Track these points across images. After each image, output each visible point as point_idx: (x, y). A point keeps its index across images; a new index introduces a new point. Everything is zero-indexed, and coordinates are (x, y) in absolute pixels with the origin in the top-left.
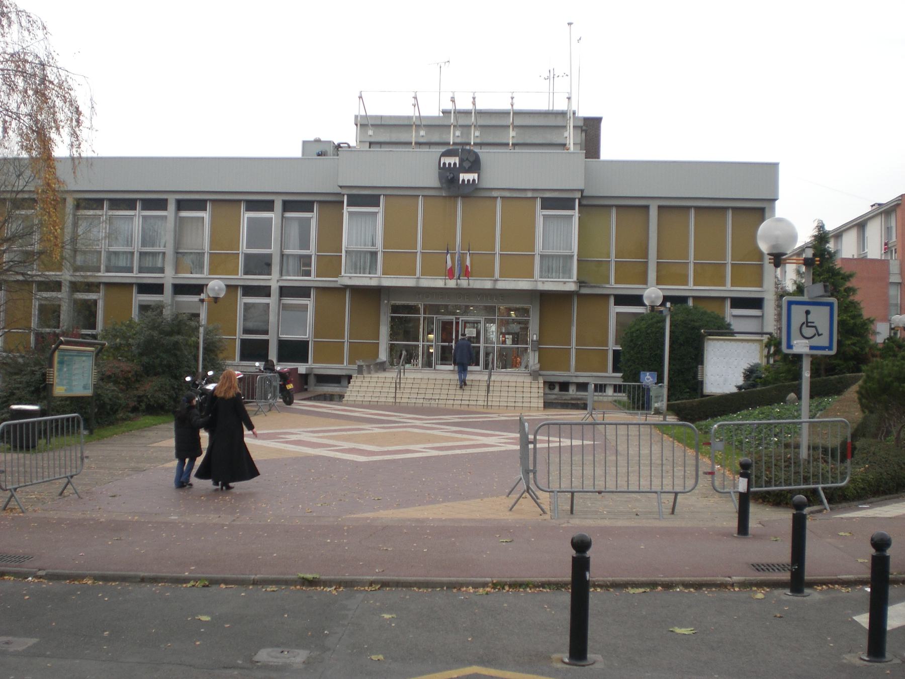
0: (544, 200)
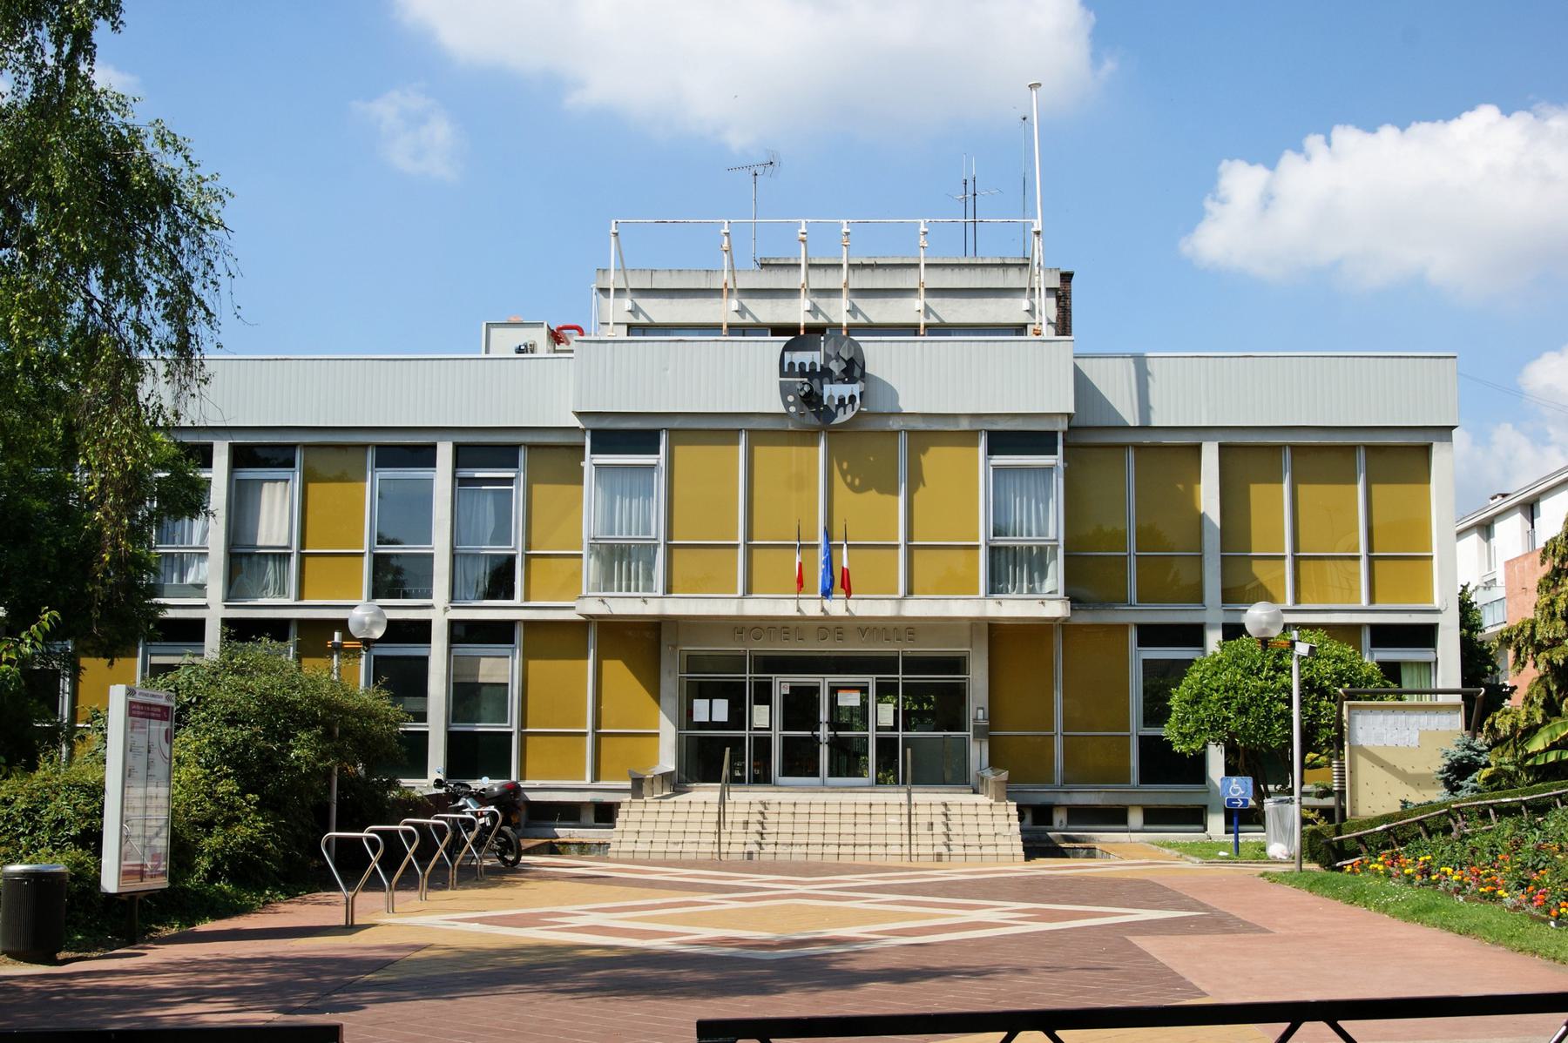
0: (992, 435)
